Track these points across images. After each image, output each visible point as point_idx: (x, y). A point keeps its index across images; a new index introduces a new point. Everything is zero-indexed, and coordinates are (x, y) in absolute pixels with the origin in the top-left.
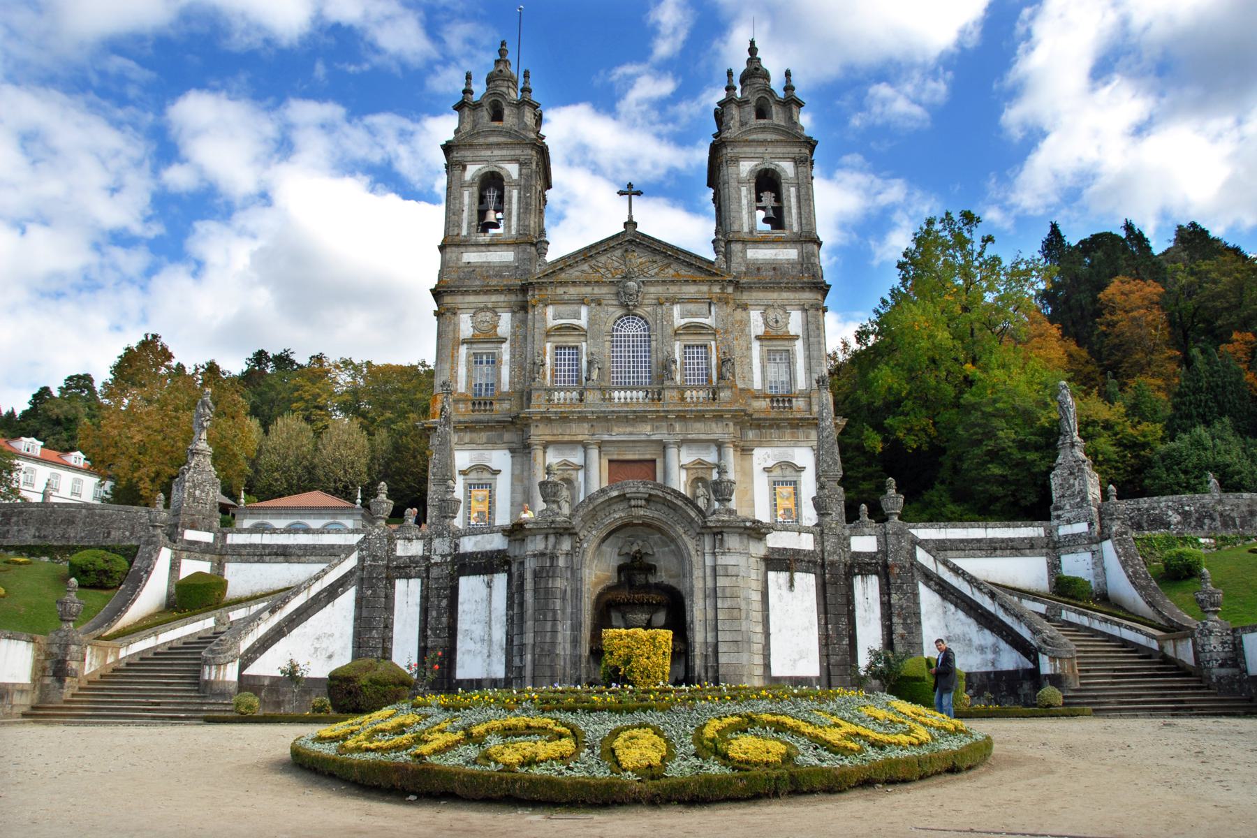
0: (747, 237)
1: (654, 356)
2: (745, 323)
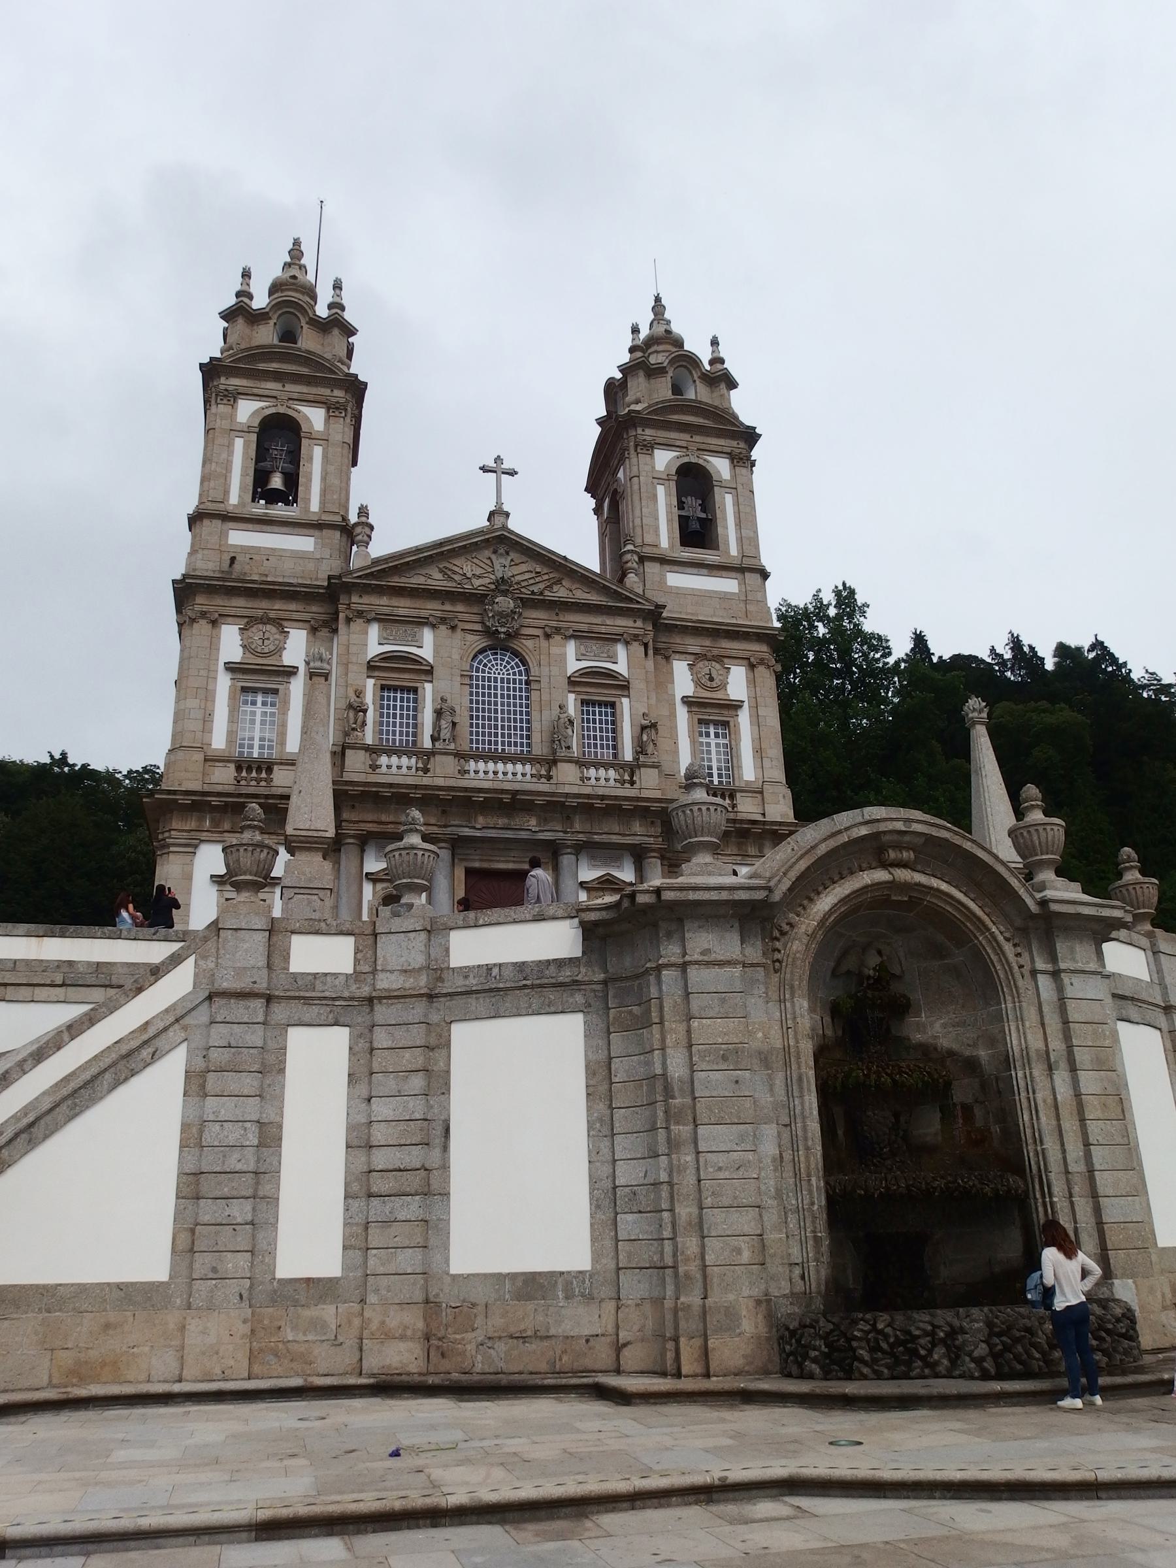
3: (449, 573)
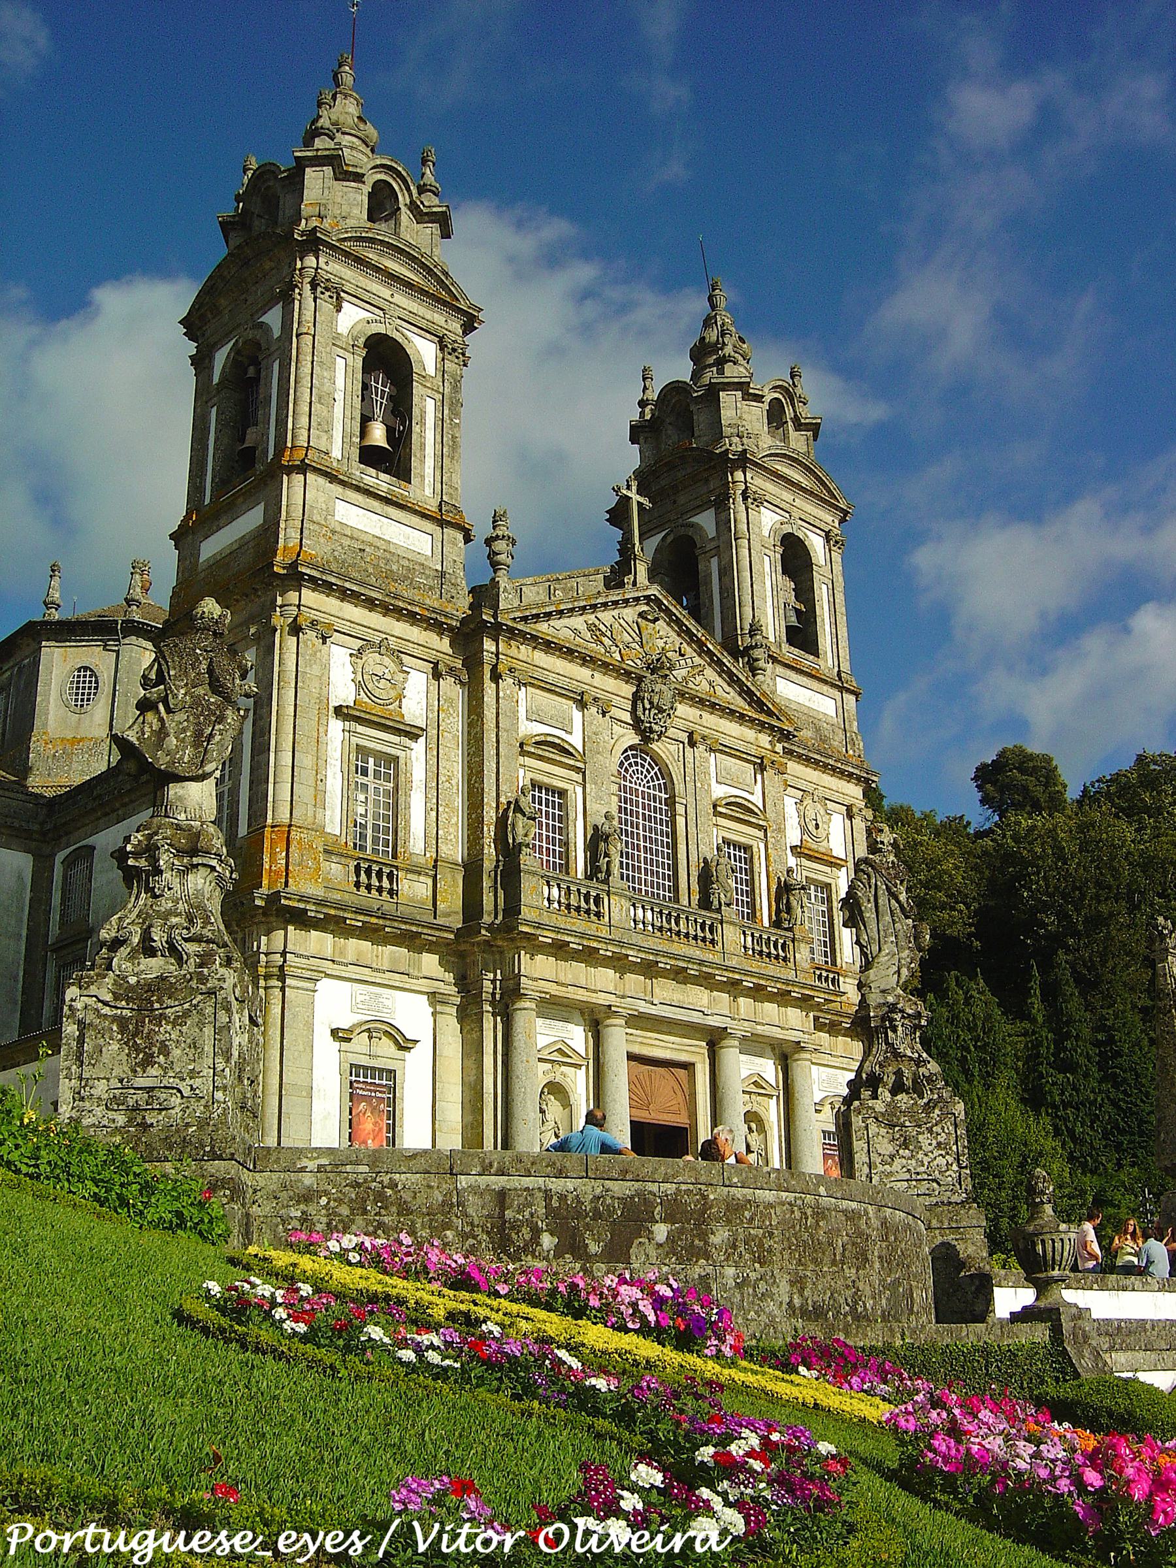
1: (682, 847)
3: (598, 633)
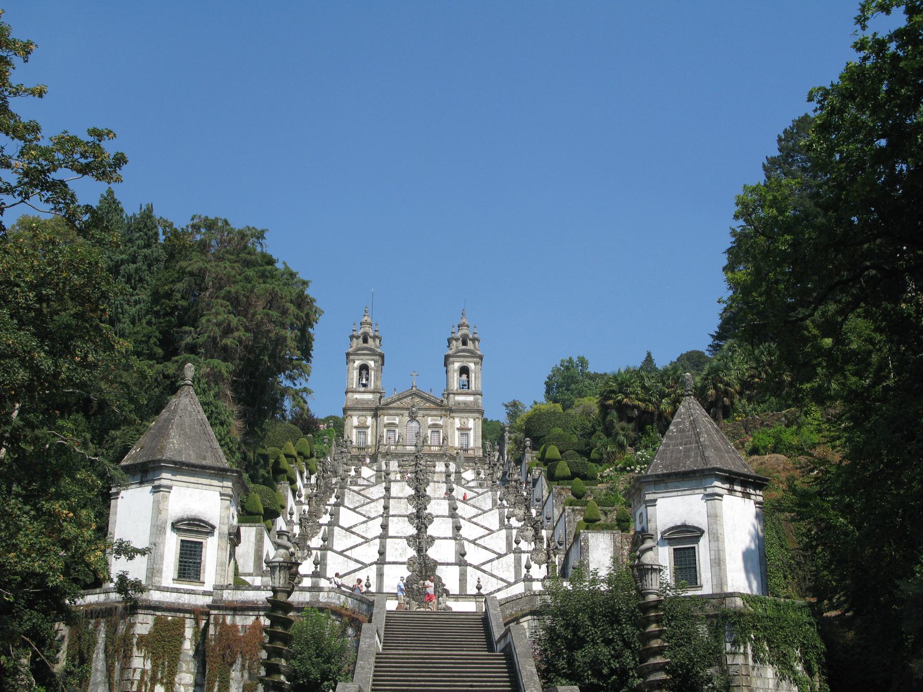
0: (455, 392)
2: (453, 424)
